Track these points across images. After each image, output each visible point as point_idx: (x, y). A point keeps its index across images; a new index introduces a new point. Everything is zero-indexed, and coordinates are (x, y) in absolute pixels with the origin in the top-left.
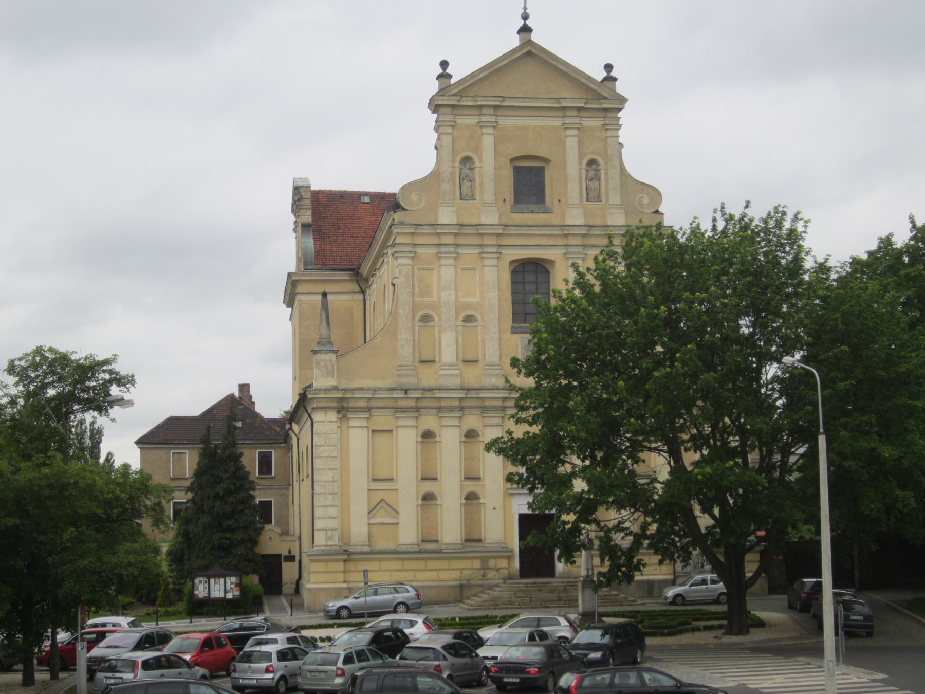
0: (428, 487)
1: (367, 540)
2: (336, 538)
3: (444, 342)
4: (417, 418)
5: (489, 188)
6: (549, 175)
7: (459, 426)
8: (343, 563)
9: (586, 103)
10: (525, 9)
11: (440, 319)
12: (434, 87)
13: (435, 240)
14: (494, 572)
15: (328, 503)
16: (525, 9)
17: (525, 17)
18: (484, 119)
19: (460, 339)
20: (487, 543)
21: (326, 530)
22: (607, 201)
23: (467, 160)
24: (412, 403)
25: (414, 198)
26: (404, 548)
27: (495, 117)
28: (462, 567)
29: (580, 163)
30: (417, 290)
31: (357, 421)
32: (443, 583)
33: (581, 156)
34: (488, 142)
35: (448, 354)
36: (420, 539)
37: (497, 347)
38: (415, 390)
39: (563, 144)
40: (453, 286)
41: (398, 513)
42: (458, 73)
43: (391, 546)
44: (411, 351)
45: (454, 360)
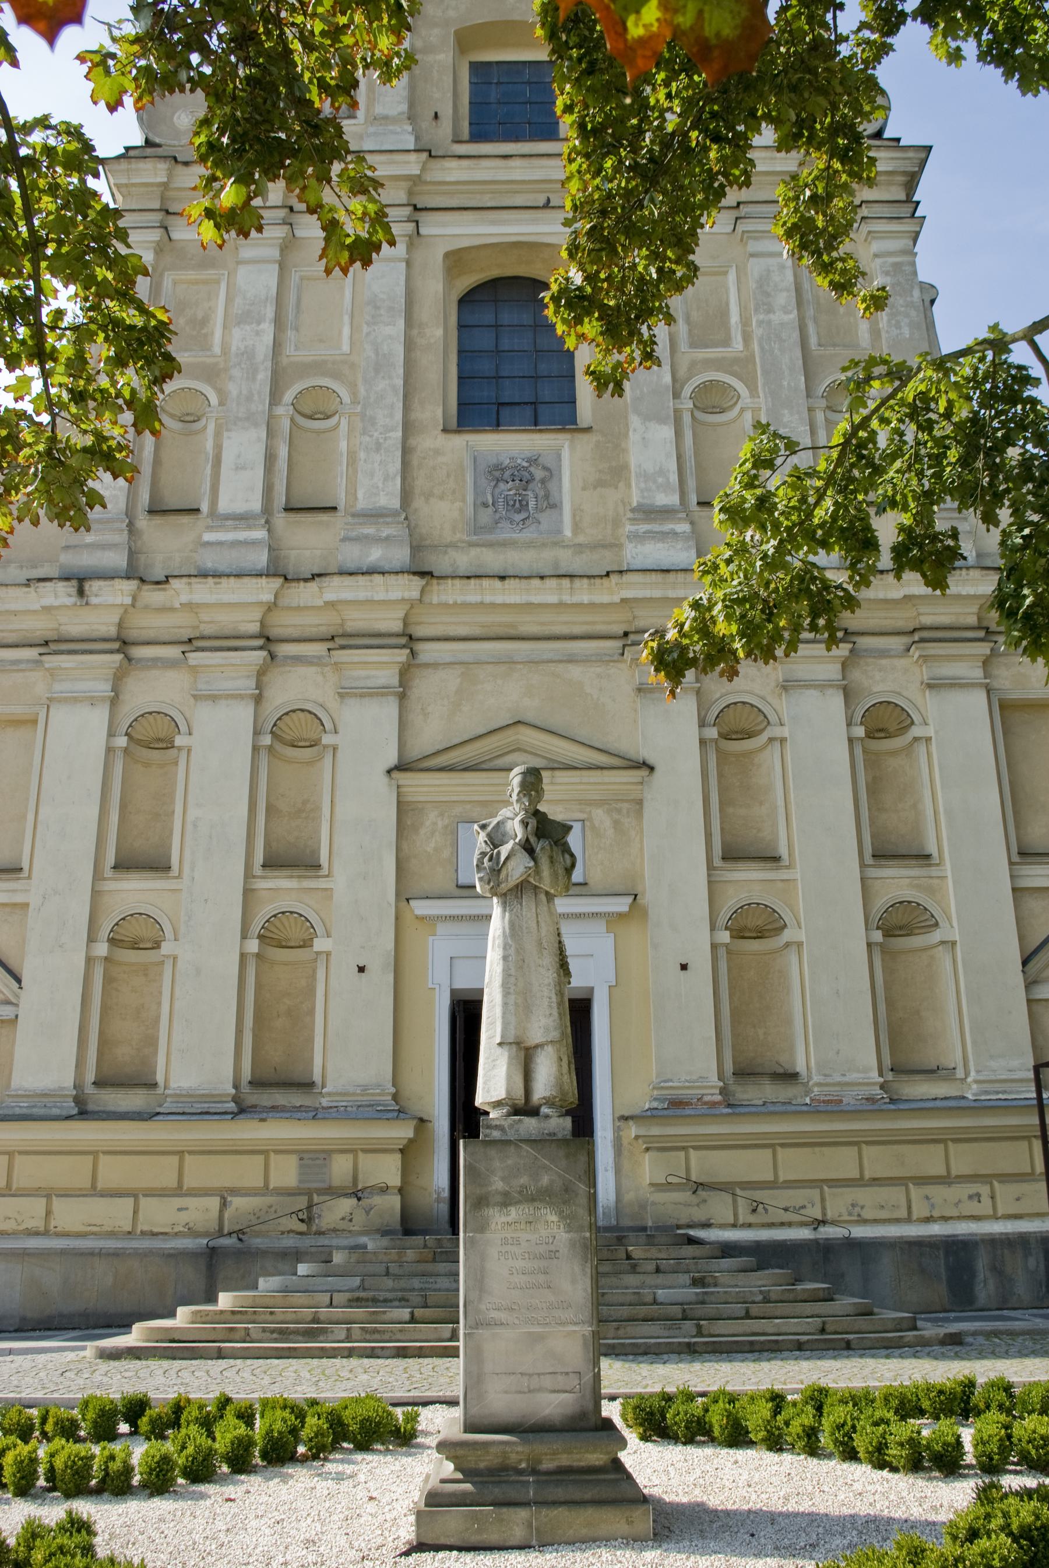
3: (228, 458)
14: (347, 1204)
20: (329, 1094)
28: (228, 1184)
32: (146, 1244)
40: (270, 312)
41: (19, 981)
45: (256, 505)
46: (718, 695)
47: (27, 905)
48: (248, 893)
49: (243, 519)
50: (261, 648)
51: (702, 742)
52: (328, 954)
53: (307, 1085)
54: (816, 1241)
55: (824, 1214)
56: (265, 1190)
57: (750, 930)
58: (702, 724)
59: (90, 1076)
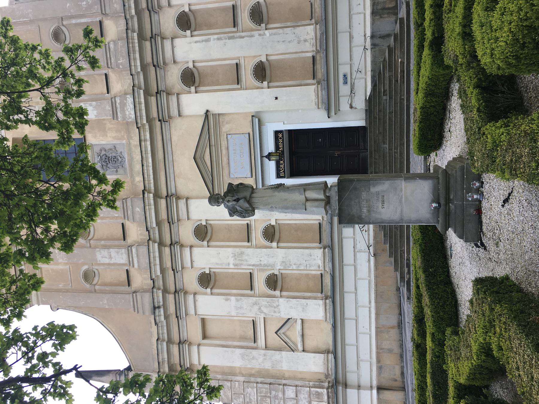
1: (323, 355)
8: (348, 390)
24: (171, 298)
26: (329, 315)
41: (289, 319)
43: (328, 327)
46: (179, 86)
47: (264, 318)
48: (257, 247)
50: (174, 246)
51: (196, 92)
52: (276, 220)
54: (372, 49)
55: (361, 46)
57: (263, 73)
58: (190, 92)
59: (319, 295)
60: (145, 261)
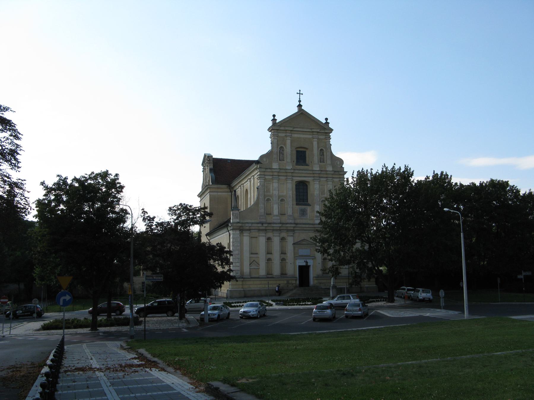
0: (269, 256)
2: (239, 273)
4: (266, 233)
5: (289, 157)
6: (307, 153)
7: (280, 236)
9: (320, 130)
10: (300, 99)
11: (273, 200)
12: (270, 124)
13: (271, 174)
14: (291, 285)
15: (236, 261)
16: (300, 99)
17: (300, 101)
18: (287, 134)
19: (280, 207)
21: (236, 271)
22: (326, 163)
23: (281, 148)
25: (265, 160)
26: (261, 277)
27: (291, 134)
29: (318, 150)
30: (265, 190)
31: (246, 234)
33: (318, 147)
34: (288, 142)
35: (276, 212)
36: (267, 274)
37: (292, 210)
38: (265, 223)
39: (312, 144)
40: (277, 189)
41: (259, 265)
42: (279, 119)
43: (257, 276)
44: (264, 210)
45: (278, 214)
49: (277, 216)
53: (286, 274)
56: (283, 284)
60: (275, 221)
